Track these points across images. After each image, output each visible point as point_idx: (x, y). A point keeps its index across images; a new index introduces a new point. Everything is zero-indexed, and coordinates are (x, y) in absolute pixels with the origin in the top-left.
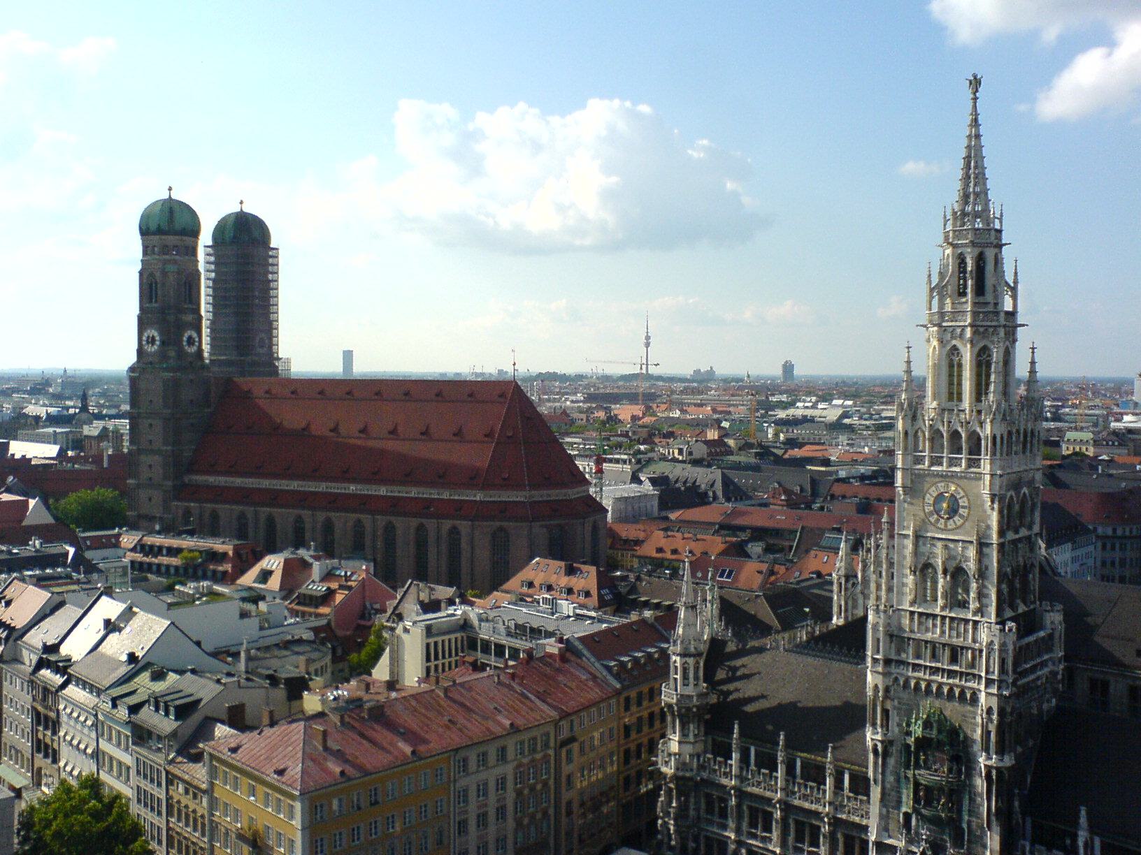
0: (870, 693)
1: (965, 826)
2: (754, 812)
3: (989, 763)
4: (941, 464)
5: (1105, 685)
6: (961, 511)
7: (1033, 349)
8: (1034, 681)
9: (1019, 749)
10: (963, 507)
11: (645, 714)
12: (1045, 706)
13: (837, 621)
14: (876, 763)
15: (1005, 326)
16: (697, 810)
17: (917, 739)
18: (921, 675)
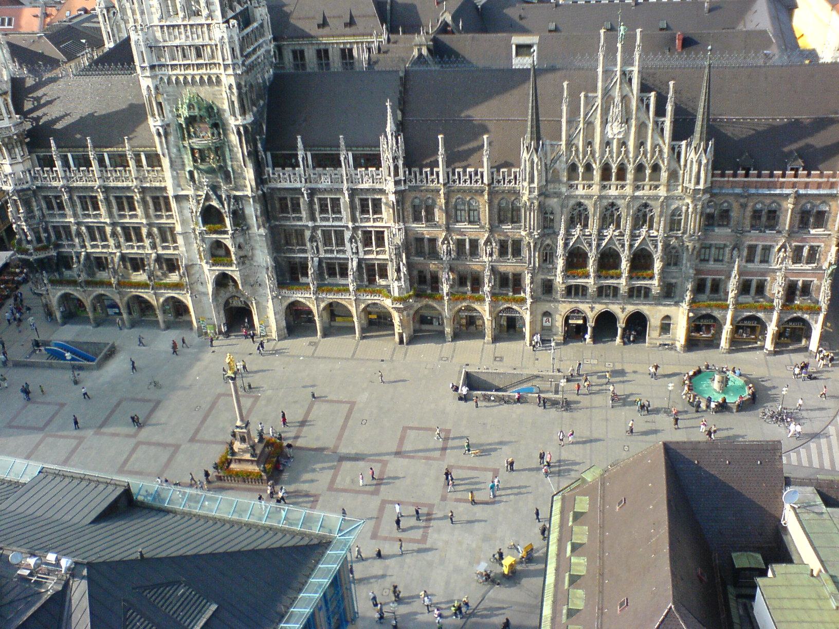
0: (145, 92)
1: (230, 169)
5: (302, 52)
8: (255, 60)
9: (255, 109)
12: (266, 76)
13: (109, 45)
14: (161, 142)
17: (186, 119)
18: (178, 72)
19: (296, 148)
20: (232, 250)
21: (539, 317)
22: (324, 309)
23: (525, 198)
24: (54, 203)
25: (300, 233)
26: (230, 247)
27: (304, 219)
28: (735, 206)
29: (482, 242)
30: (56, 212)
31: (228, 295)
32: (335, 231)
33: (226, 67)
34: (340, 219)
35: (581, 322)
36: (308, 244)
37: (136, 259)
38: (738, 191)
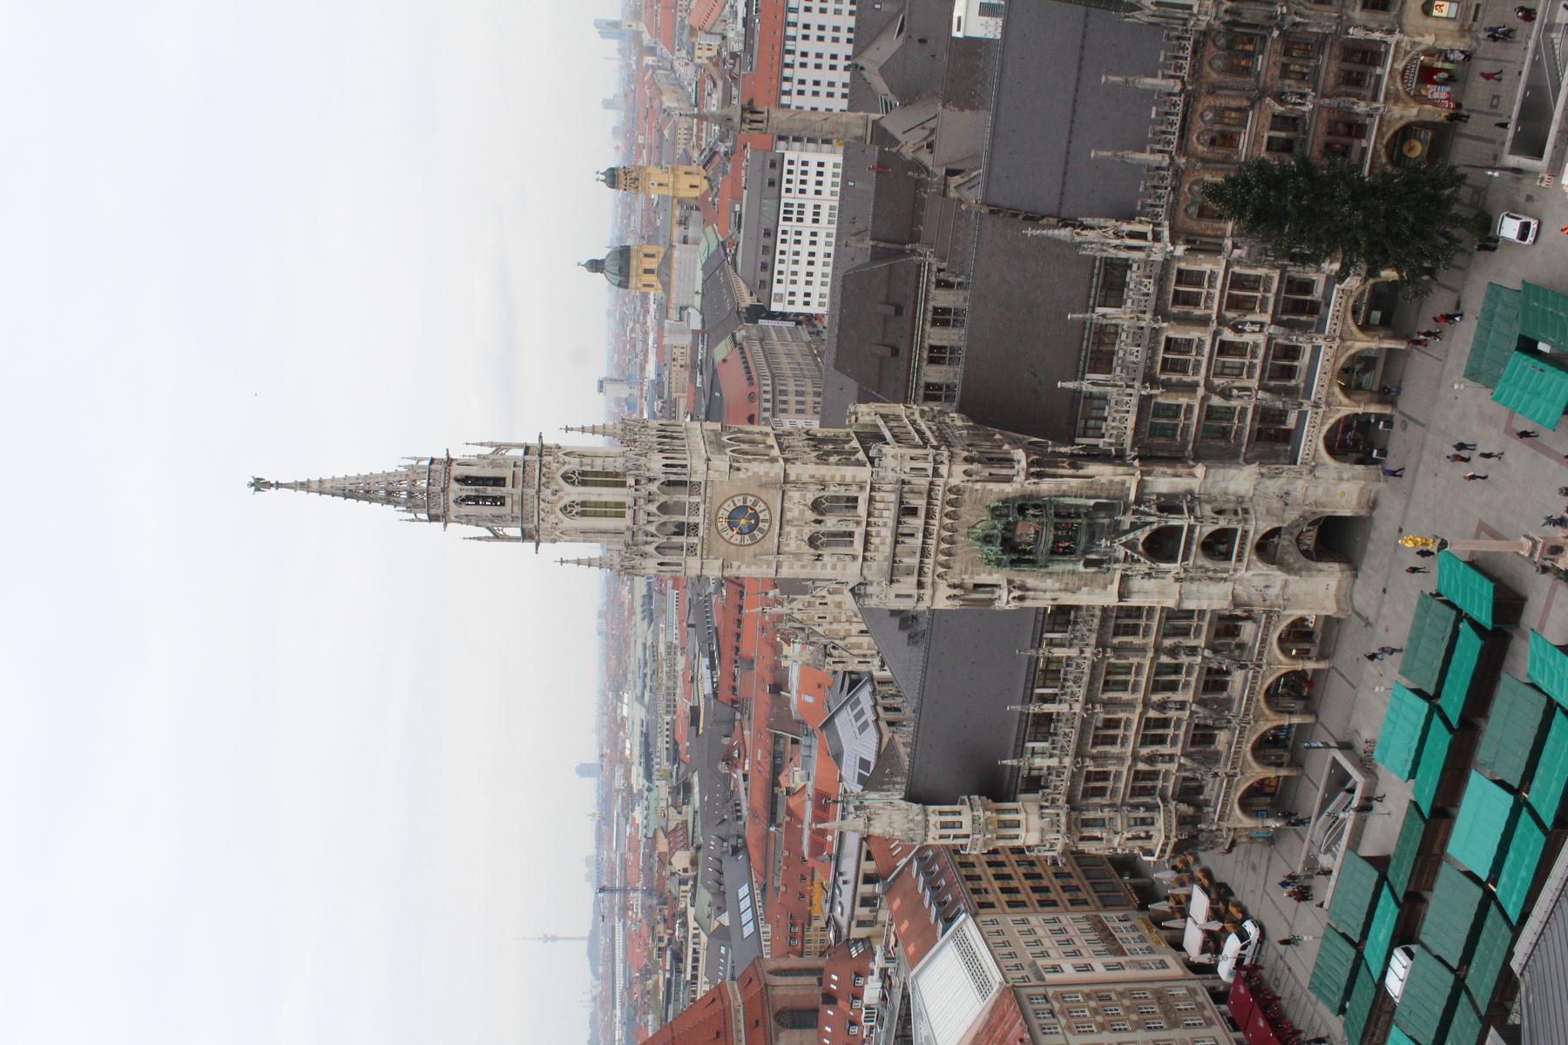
1: (1092, 502)
2: (1100, 740)
3: (1022, 476)
4: (696, 525)
5: (928, 385)
7: (567, 429)
9: (1006, 447)
10: (745, 501)
11: (997, 884)
12: (959, 423)
15: (540, 455)
16: (1102, 806)
17: (1003, 552)
18: (932, 549)
20: (1223, 523)
23: (1216, 24)
24: (1093, 784)
25: (1210, 413)
26: (1217, 527)
27: (1191, 402)
29: (1279, 109)
30: (1109, 784)
31: (1293, 549)
32: (1220, 353)
33: (936, 473)
34: (1201, 342)
36: (1234, 403)
37: (1206, 683)
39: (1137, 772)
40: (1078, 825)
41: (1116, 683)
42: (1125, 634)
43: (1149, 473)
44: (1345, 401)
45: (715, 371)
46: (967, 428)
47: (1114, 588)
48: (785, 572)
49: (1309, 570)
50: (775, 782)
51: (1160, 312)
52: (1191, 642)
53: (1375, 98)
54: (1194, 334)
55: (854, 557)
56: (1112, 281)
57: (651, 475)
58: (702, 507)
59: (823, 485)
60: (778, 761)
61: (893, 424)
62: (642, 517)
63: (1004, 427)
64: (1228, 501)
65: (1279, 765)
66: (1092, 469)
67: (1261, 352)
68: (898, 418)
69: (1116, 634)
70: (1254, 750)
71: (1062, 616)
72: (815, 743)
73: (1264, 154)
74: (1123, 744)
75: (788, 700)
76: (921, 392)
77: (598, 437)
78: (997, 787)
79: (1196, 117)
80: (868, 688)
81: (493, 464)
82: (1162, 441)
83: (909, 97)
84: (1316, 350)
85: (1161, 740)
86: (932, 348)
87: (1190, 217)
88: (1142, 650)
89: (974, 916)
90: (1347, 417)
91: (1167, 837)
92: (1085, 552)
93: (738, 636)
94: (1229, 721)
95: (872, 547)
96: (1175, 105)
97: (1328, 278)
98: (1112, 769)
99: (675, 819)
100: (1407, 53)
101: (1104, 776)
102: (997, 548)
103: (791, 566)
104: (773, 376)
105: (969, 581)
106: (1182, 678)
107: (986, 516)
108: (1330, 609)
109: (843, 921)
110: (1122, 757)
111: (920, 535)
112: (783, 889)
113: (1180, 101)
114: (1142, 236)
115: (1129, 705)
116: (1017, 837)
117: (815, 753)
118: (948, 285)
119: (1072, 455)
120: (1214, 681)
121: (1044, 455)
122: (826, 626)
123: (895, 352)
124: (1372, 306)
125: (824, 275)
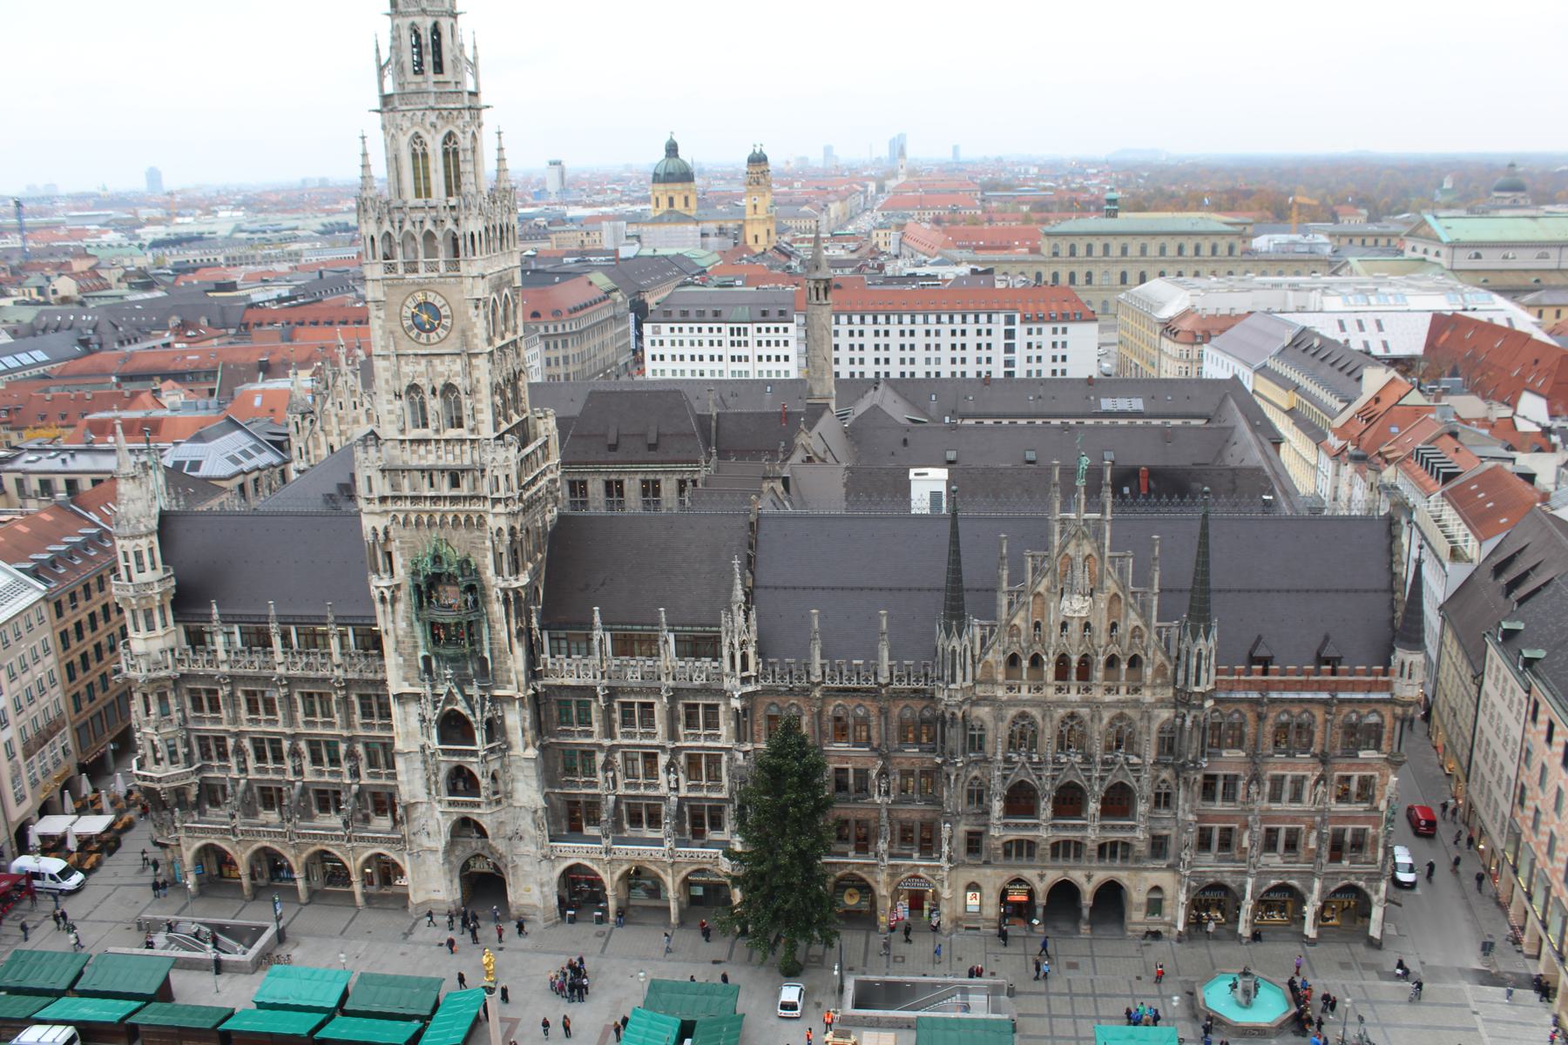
0: (369, 537)
1: (487, 655)
3: (503, 585)
4: (416, 271)
5: (584, 483)
6: (444, 321)
9: (530, 566)
11: (84, 617)
12: (548, 517)
15: (470, 108)
16: (183, 710)
18: (421, 506)
19: (591, 626)
20: (484, 782)
21: (961, 891)
22: (621, 878)
23: (941, 707)
24: (205, 698)
25: (588, 754)
28: (1250, 716)
29: (873, 774)
30: (207, 714)
31: (469, 852)
32: (646, 755)
33: (496, 501)
35: (1024, 898)
36: (600, 774)
37: (325, 792)
38: (1255, 695)
39: (224, 739)
40: (160, 690)
41: (312, 704)
42: (362, 706)
43: (522, 706)
44: (616, 877)
45: (579, 274)
46: (544, 525)
47: (407, 689)
48: (379, 365)
49: (451, 871)
50: (165, 376)
51: (676, 693)
52: (363, 771)
53: (892, 856)
54: (660, 727)
55: (402, 431)
56: (701, 645)
57: (462, 221)
58: (435, 274)
59: (471, 393)
60: (189, 378)
61: (540, 454)
62: (418, 215)
63: (551, 561)
64: (506, 784)
65: (252, 876)
66: (519, 651)
67: (651, 792)
68: (546, 458)
69: (361, 697)
70: (264, 849)
71: (372, 642)
72: (212, 413)
73: (831, 767)
74: (250, 720)
75: (254, 380)
76: (577, 477)
77: (495, 166)
78: (187, 602)
79: (858, 701)
80: (276, 460)
81: (456, 61)
82: (555, 714)
83: (853, 434)
84: (659, 842)
85: (261, 757)
86: (620, 483)
87: (768, 708)
88: (349, 724)
89: (45, 599)
90: (601, 881)
91: (160, 780)
92: (437, 656)
93: (316, 323)
94: (289, 820)
95: (415, 447)
96: (867, 680)
97: (728, 842)
98: (224, 714)
99: (111, 276)
100: (933, 876)
101: (215, 707)
102: (430, 569)
103: (386, 370)
104: (580, 332)
105: (394, 547)
106: (327, 768)
107: (460, 555)
108: (416, 898)
109: (19, 464)
110: (235, 722)
111: (433, 493)
112: (48, 397)
113: (871, 684)
114: (745, 667)
115: (291, 721)
116: (137, 630)
117: (202, 414)
118: (681, 491)
119: (530, 630)
120: (327, 799)
121: (527, 602)
122: (333, 411)
123: (613, 448)
124: (708, 887)
125: (682, 372)
